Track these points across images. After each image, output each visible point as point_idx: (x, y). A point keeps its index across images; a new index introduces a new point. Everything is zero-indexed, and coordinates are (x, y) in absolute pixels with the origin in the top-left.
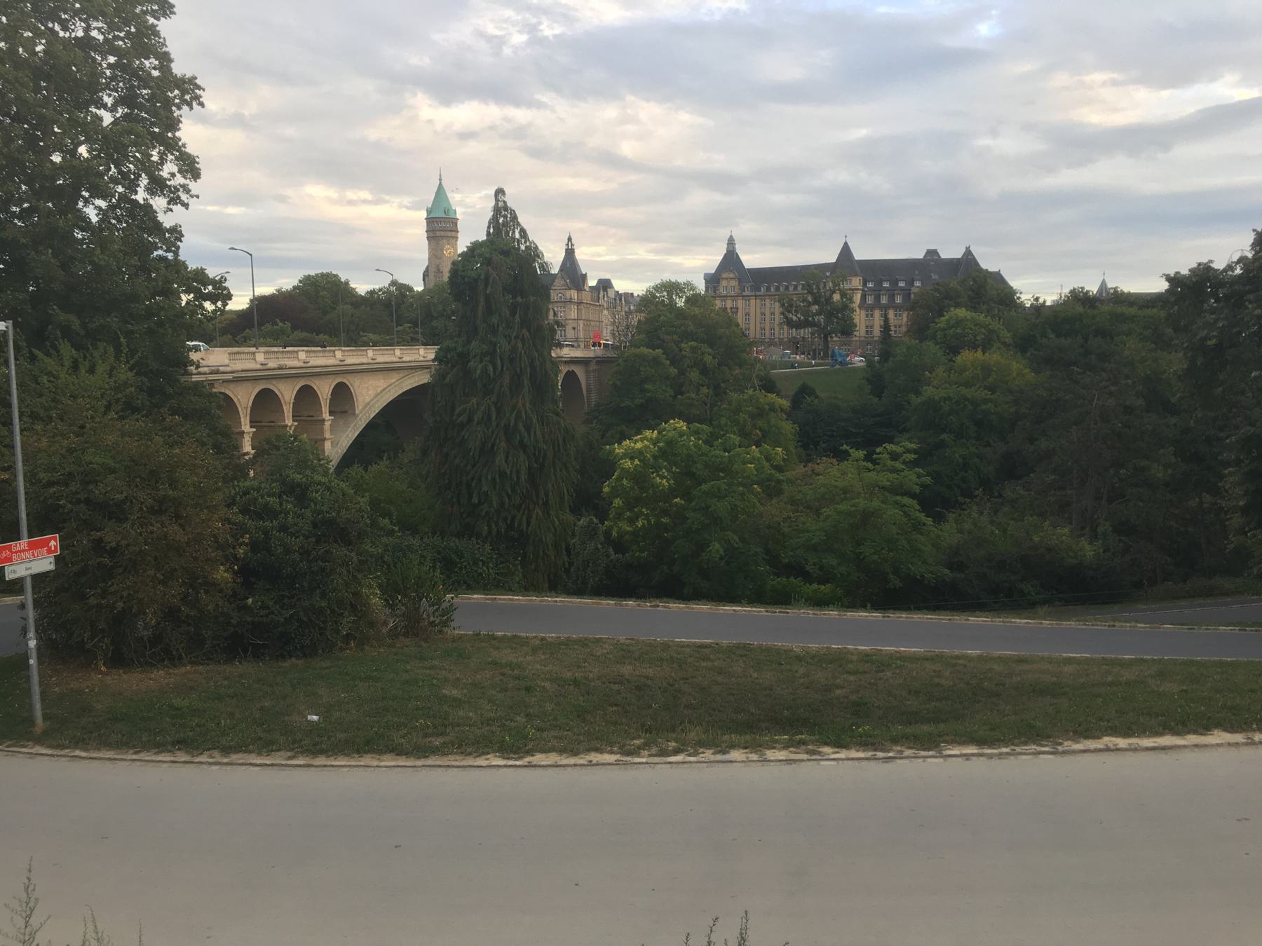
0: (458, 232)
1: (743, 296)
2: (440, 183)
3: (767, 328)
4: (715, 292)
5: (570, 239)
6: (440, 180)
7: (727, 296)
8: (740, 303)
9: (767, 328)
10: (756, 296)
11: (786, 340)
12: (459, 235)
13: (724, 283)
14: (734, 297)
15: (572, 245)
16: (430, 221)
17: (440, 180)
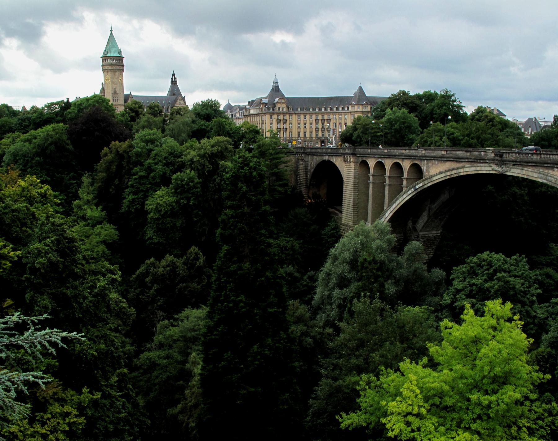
0: (123, 66)
1: (289, 113)
2: (111, 33)
3: (308, 131)
4: (273, 110)
5: (174, 75)
6: (111, 31)
7: (280, 113)
8: (287, 117)
9: (308, 131)
10: (295, 113)
11: (314, 139)
12: (124, 68)
13: (279, 105)
14: (284, 114)
15: (175, 78)
16: (104, 58)
17: (111, 31)
